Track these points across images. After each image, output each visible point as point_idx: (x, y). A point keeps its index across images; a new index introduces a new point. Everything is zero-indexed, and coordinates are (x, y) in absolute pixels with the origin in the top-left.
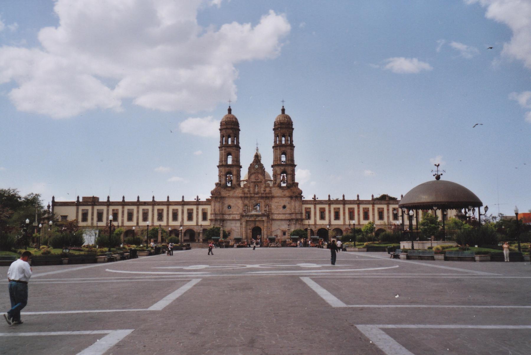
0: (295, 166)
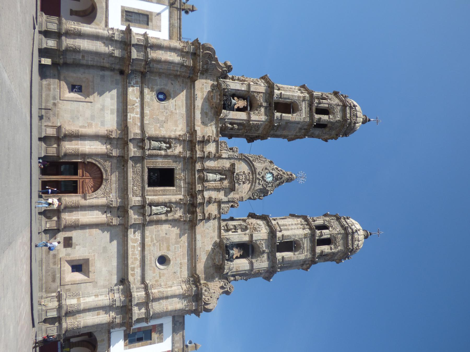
0: (268, 278)
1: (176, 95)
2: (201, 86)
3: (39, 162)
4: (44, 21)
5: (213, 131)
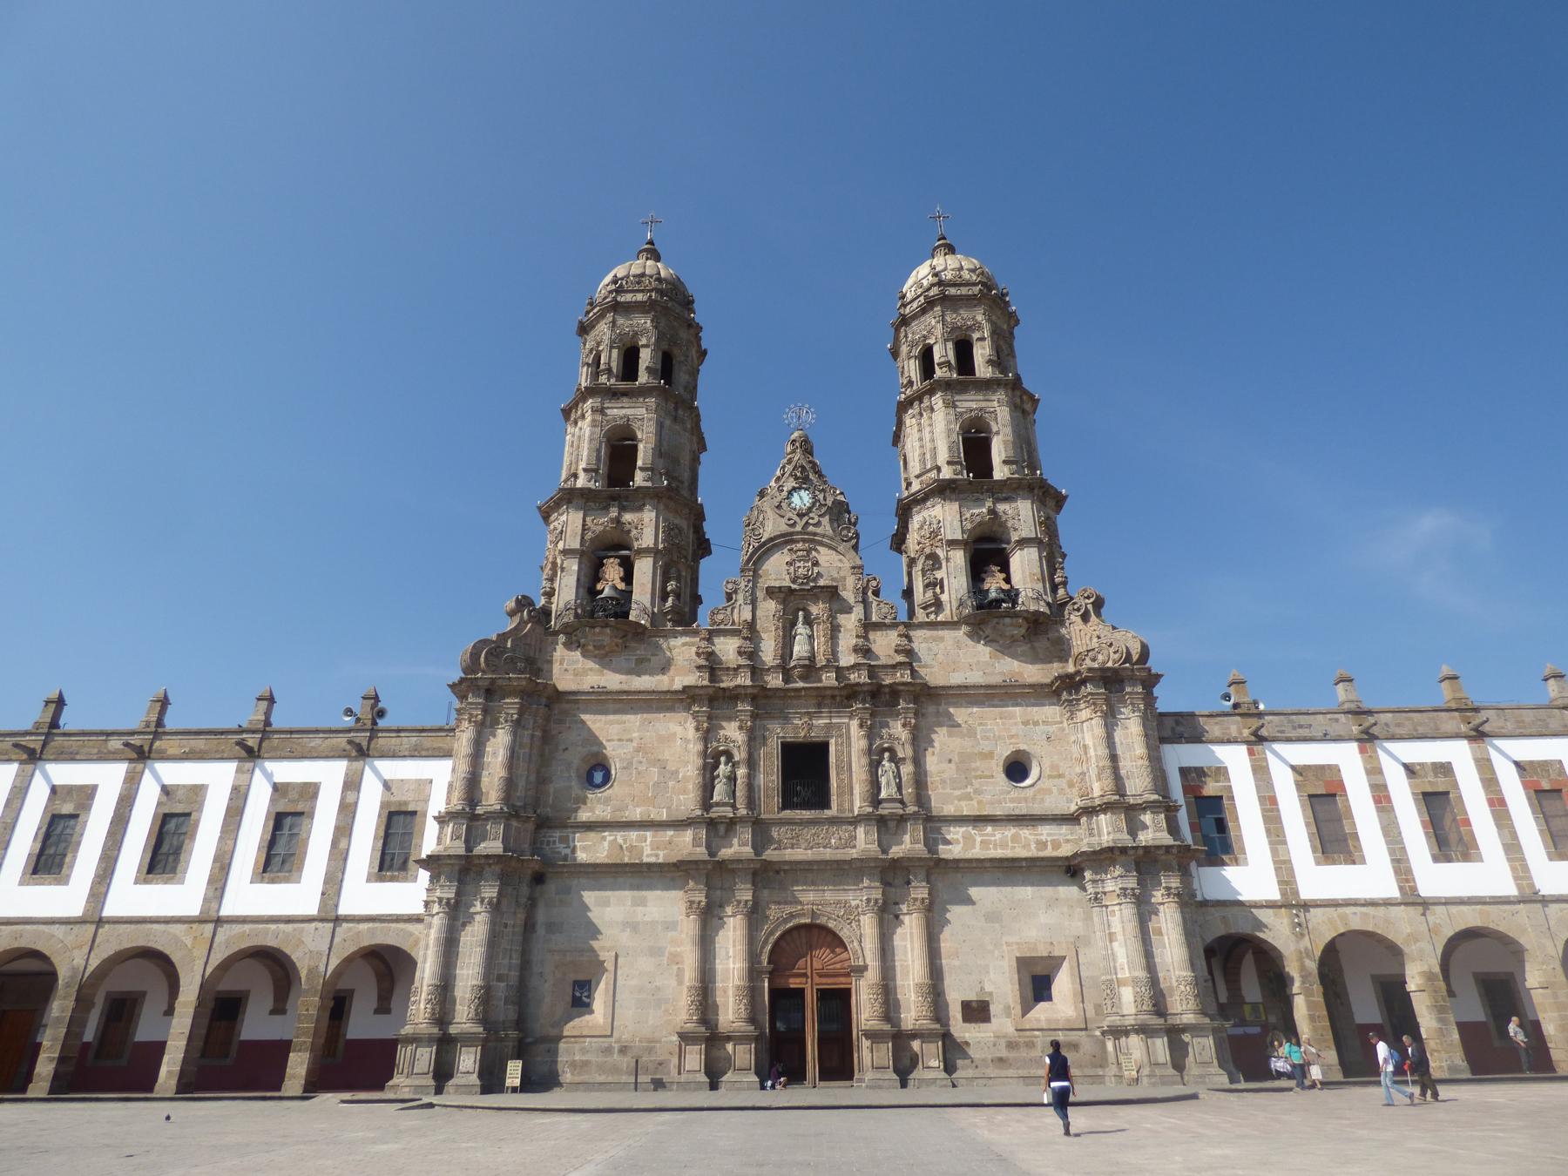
0: (1060, 501)
1: (592, 739)
2: (569, 677)
3: (773, 1087)
4: (408, 1082)
5: (684, 644)
